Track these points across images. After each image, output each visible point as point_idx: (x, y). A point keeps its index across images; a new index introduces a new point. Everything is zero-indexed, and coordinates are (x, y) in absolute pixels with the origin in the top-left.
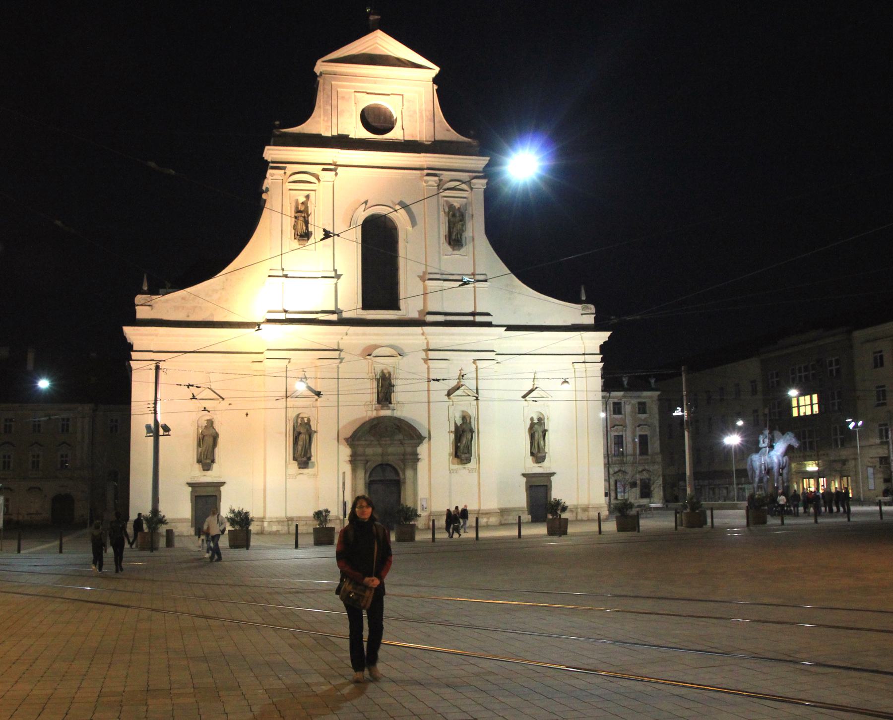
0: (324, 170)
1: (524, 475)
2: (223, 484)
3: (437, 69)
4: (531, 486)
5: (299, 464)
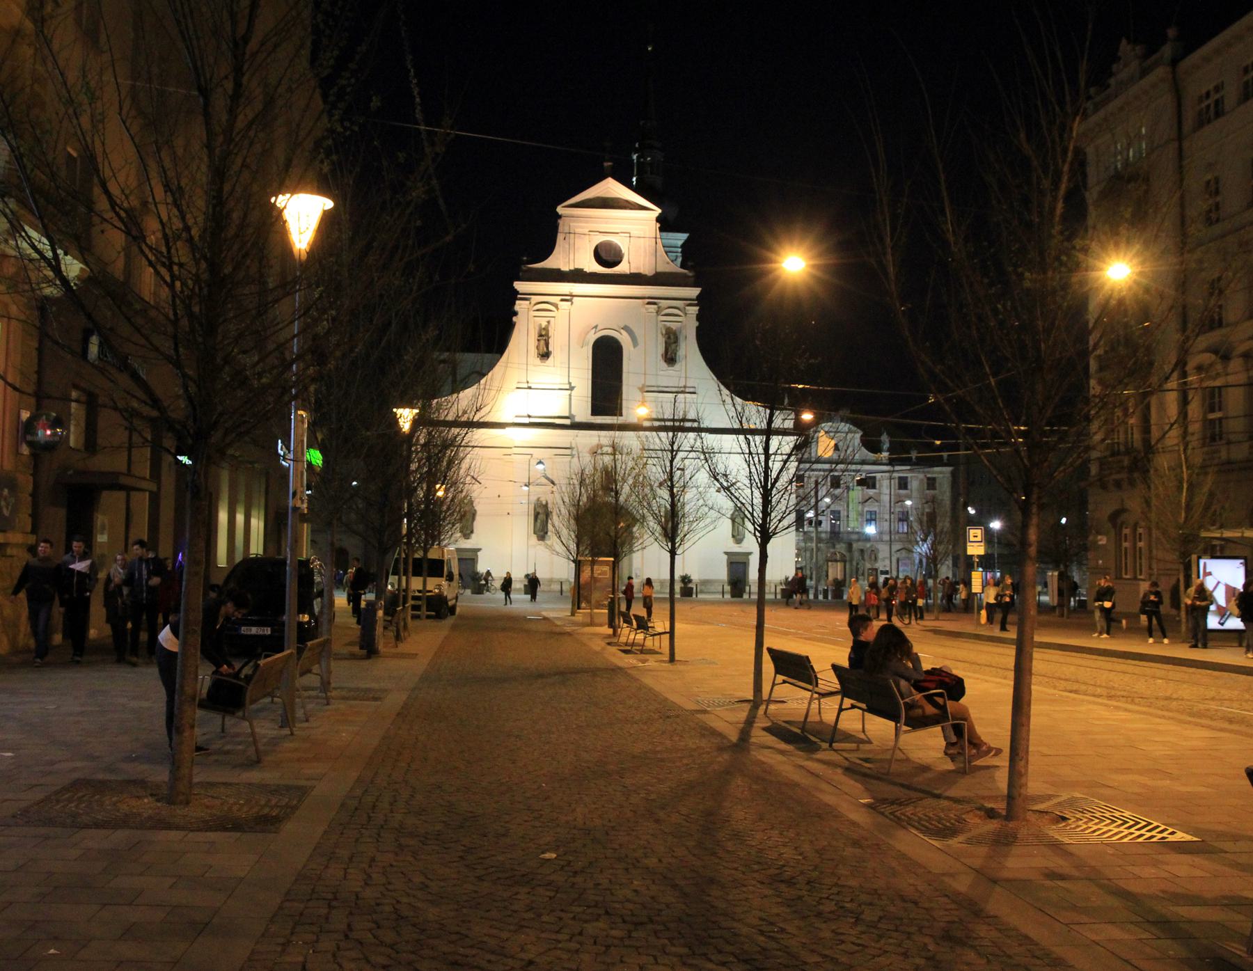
0: (562, 300)
1: (726, 553)
2: (479, 550)
3: (659, 211)
4: (731, 563)
5: (538, 537)
